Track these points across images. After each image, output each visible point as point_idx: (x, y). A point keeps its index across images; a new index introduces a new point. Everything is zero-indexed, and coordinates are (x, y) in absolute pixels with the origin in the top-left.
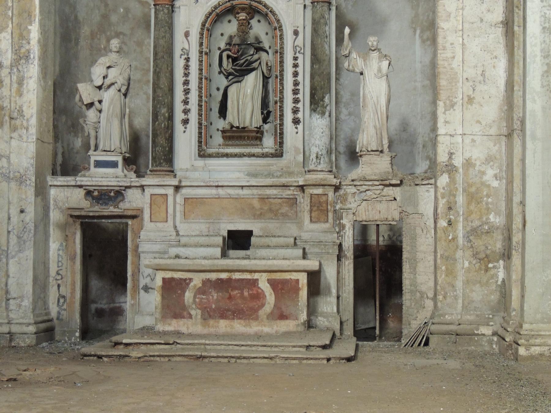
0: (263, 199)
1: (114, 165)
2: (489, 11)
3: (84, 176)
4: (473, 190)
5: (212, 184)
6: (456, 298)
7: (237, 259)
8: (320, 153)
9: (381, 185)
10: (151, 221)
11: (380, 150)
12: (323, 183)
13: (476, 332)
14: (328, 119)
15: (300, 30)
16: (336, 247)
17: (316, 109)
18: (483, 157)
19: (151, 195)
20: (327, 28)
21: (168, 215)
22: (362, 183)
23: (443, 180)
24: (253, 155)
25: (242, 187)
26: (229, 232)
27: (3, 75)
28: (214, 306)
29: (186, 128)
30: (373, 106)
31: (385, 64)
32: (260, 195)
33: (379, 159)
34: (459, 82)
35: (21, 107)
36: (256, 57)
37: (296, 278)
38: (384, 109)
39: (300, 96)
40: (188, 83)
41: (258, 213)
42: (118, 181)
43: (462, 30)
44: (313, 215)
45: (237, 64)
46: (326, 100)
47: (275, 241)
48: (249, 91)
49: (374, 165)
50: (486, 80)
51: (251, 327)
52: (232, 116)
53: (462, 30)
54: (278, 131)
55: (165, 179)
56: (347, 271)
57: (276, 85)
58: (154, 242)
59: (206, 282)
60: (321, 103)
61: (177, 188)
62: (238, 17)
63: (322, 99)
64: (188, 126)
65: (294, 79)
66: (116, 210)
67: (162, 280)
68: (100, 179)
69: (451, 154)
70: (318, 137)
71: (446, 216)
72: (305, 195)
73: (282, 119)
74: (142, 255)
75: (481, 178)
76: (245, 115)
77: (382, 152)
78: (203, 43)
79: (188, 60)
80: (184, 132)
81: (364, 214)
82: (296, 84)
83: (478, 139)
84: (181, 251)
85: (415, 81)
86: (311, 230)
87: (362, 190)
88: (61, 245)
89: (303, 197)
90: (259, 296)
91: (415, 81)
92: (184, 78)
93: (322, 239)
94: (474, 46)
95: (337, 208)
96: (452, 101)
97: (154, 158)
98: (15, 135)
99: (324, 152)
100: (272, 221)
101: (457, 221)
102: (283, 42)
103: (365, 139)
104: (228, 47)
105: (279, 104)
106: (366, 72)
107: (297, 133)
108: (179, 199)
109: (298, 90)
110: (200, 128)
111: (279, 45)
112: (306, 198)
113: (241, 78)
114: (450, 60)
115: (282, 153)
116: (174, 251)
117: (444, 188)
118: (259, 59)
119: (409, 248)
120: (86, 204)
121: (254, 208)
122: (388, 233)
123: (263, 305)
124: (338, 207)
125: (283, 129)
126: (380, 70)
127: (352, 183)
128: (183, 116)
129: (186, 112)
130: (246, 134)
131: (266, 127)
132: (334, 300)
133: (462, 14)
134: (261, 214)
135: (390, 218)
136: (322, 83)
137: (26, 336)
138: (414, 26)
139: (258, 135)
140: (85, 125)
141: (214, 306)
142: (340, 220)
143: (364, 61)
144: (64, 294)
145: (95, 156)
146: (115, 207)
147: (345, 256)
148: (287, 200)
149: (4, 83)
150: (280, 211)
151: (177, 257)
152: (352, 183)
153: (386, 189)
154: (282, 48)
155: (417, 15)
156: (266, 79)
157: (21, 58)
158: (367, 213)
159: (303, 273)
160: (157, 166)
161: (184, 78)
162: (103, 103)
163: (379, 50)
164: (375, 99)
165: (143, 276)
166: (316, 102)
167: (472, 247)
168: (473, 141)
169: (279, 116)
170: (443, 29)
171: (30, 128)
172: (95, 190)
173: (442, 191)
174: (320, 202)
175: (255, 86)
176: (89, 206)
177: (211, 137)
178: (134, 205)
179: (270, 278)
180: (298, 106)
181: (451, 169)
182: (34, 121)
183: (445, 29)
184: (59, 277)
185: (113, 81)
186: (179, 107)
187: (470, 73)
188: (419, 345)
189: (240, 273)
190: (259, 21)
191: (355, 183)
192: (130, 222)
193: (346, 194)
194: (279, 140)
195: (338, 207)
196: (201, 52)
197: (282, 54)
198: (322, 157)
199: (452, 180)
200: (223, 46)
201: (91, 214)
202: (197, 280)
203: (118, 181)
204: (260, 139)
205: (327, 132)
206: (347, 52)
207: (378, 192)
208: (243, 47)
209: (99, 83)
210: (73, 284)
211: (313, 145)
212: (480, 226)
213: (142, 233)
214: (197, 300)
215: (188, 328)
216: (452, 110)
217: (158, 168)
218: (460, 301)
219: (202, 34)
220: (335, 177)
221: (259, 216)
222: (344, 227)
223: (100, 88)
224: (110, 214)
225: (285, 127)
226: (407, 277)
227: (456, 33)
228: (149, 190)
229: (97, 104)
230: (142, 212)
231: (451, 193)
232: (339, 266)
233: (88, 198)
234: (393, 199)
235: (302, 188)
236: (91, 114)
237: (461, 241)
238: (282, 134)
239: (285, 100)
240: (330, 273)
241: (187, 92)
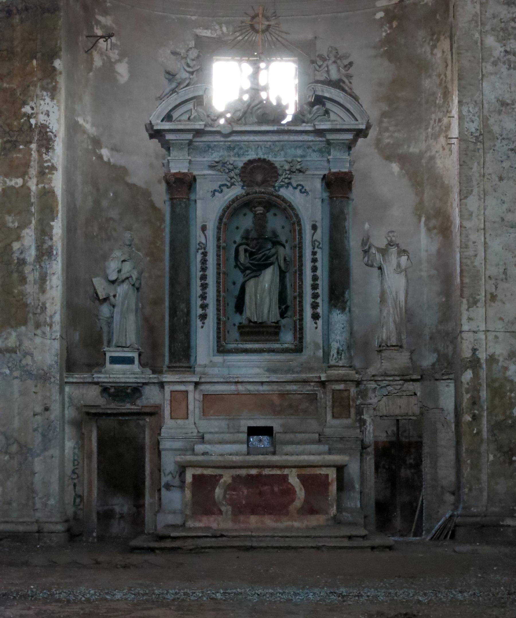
0: (283, 395)
1: (129, 361)
2: (510, 211)
3: (100, 372)
4: (497, 385)
5: (231, 380)
6: (481, 490)
8: (341, 349)
9: (401, 380)
10: (171, 418)
12: (345, 378)
13: (501, 523)
14: (348, 314)
15: (318, 224)
16: (359, 442)
18: (505, 353)
19: (171, 391)
21: (189, 412)
23: (468, 375)
25: (262, 383)
27: (26, 272)
28: (244, 502)
29: (203, 323)
32: (279, 391)
33: (398, 354)
34: (481, 279)
35: (44, 304)
36: (273, 251)
37: (326, 473)
40: (206, 278)
42: (136, 378)
43: (484, 229)
44: (335, 410)
48: (267, 286)
49: (394, 361)
50: (508, 278)
51: (281, 522)
52: (250, 312)
53: (484, 229)
54: (298, 326)
55: (186, 376)
57: (295, 279)
59: (236, 478)
60: (342, 298)
62: (256, 211)
64: (206, 321)
66: (133, 407)
67: (191, 476)
69: (474, 350)
70: (339, 333)
71: (471, 410)
73: (301, 315)
74: (163, 453)
75: (504, 373)
77: (401, 347)
78: (220, 237)
79: (205, 254)
80: (202, 327)
81: (384, 409)
82: (315, 278)
83: (501, 335)
85: (421, 270)
86: (334, 425)
88: (77, 443)
89: (325, 393)
90: (290, 491)
91: (421, 270)
92: (201, 273)
94: (496, 245)
96: (474, 298)
97: (172, 355)
98: (39, 332)
99: (345, 348)
100: (293, 417)
101: (481, 416)
102: (302, 237)
104: (244, 241)
105: (298, 299)
107: (316, 328)
108: (199, 396)
109: (318, 285)
110: (218, 324)
111: (297, 240)
112: (328, 394)
114: (472, 258)
115: (302, 348)
117: (468, 384)
120: (101, 401)
123: (293, 500)
125: (302, 324)
126: (399, 265)
127: (372, 378)
128: (200, 311)
129: (204, 307)
130: (265, 329)
131: (284, 322)
132: (358, 496)
133: (484, 213)
135: (410, 413)
137: (53, 535)
138: (418, 213)
139: (276, 330)
140: (97, 320)
141: (244, 502)
143: (383, 256)
144: (80, 493)
145: (112, 352)
146: (132, 405)
149: (28, 280)
150: (300, 407)
152: (372, 378)
153: (406, 385)
154: (301, 243)
155: (421, 202)
157: (43, 255)
158: (387, 408)
159: (333, 469)
160: (175, 362)
161: (201, 273)
164: (394, 294)
165: (164, 474)
167: (496, 440)
168: (496, 337)
169: (298, 311)
170: (466, 227)
171: (54, 325)
172: (112, 386)
173: (467, 386)
176: (105, 403)
177: (228, 332)
178: (152, 402)
179: (300, 473)
181: (474, 363)
182: (57, 318)
183: (467, 228)
184: (75, 476)
185: (128, 275)
186: (196, 302)
187: (493, 271)
188: (446, 537)
189: (270, 469)
190: (275, 215)
193: (366, 390)
194: (298, 336)
195: (358, 402)
196: (218, 247)
197: (301, 248)
198: (343, 352)
199: (476, 375)
200: (238, 239)
201: (109, 412)
202: (227, 477)
203: (136, 378)
204: (277, 334)
207: (399, 387)
208: (260, 241)
209: (113, 276)
210: (90, 483)
211: (334, 340)
212: (504, 420)
214: (227, 496)
215: (218, 524)
216: (475, 306)
217: (178, 364)
218: (485, 494)
219: (219, 228)
220: (356, 373)
221: (278, 411)
223: (113, 282)
224: (128, 411)
227: (478, 231)
228: (168, 386)
229: (112, 298)
230: (160, 409)
231: (475, 388)
232: (361, 461)
234: (413, 394)
235: (323, 384)
236: (105, 309)
237: (485, 435)
238: (301, 329)
240: (354, 469)
241: (204, 286)
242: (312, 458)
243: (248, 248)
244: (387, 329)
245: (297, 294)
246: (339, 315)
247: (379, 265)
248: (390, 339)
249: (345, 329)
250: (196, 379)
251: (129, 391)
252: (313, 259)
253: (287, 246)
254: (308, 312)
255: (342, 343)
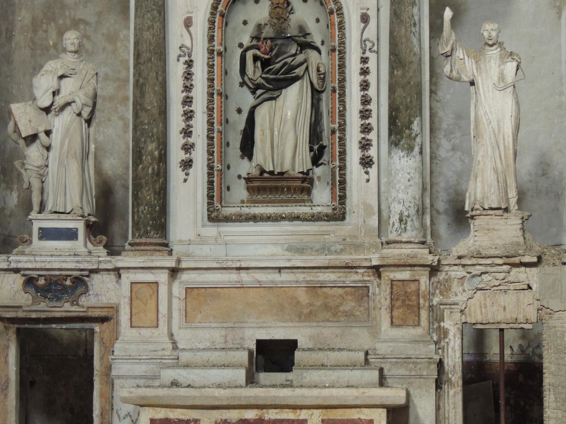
0: (313, 288)
1: (71, 235)
3: (23, 253)
5: (230, 264)
7: (272, 387)
8: (406, 214)
10: (131, 327)
11: (503, 207)
12: (410, 261)
14: (418, 158)
15: (372, 14)
16: (434, 367)
17: (399, 141)
19: (132, 283)
20: (415, 10)
21: (160, 316)
22: (474, 261)
24: (297, 218)
25: (280, 269)
26: (260, 343)
29: (187, 174)
30: (492, 136)
31: (511, 66)
32: (308, 282)
33: (502, 222)
36: (300, 58)
37: (369, 418)
38: (510, 140)
39: (372, 121)
40: (191, 102)
41: (306, 311)
42: (78, 262)
44: (395, 313)
45: (270, 70)
46: (415, 126)
47: (333, 356)
48: (289, 114)
49: (495, 232)
52: (262, 155)
54: (338, 178)
55: (154, 258)
56: (452, 406)
57: (333, 103)
58: (138, 360)
60: (407, 131)
61: (174, 272)
63: (409, 125)
64: (191, 171)
65: (362, 93)
66: (74, 308)
68: (49, 259)
70: (403, 187)
72: (383, 282)
73: (343, 159)
74: (116, 382)
76: (283, 152)
77: (506, 210)
78: (213, 36)
79: (189, 64)
80: (185, 181)
82: (366, 101)
84: (181, 375)
86: (393, 339)
87: (475, 273)
89: (379, 285)
92: (185, 94)
93: (411, 353)
95: (435, 302)
97: (136, 224)
99: (412, 211)
103: (479, 190)
104: (254, 43)
105: (337, 135)
106: (479, 81)
107: (368, 181)
108: (178, 289)
110: (210, 174)
111: (337, 38)
112: (383, 287)
113: (276, 93)
115: (344, 213)
116: (169, 375)
118: (306, 61)
119: (553, 368)
120: (24, 299)
121: (298, 302)
122: (520, 342)
124: (436, 301)
125: (345, 174)
126: (502, 77)
127: (458, 262)
128: (183, 156)
129: (188, 148)
130: (285, 184)
131: (318, 171)
134: (311, 312)
135: (521, 319)
136: (409, 100)
138: (558, 4)
139: (305, 185)
140: (23, 171)
142: (439, 322)
146: (72, 304)
147: (449, 380)
148: (353, 290)
150: (341, 309)
151: (175, 384)
153: (515, 270)
154: (342, 43)
156: (316, 93)
158: (484, 310)
160: (140, 236)
161: (185, 94)
162: (53, 135)
163: (501, 44)
164: (494, 124)
165: (119, 416)
166: (399, 131)
169: (338, 154)
172: (40, 276)
174: (406, 293)
175: (299, 105)
176: (30, 302)
177: (228, 189)
178: (104, 300)
179: (326, 418)
180: (369, 137)
185: (69, 99)
186: (176, 141)
189: (277, 411)
191: (464, 261)
192: (97, 328)
193: (448, 280)
194: (338, 193)
195: (436, 301)
197: (342, 53)
198: (409, 220)
200: (246, 41)
201: (34, 316)
203: (78, 262)
204: (308, 191)
205: (417, 179)
206: (448, 49)
207: (502, 275)
208: (279, 42)
209: (46, 103)
213: (117, 346)
217: (143, 240)
219: (212, 22)
220: (430, 253)
221: (306, 316)
222: (445, 333)
223: (47, 110)
224: (64, 314)
225: (348, 172)
226: (552, 415)
228: (127, 275)
229: (42, 136)
230: (117, 311)
232: (438, 398)
233: (28, 289)
234: (526, 287)
235: (377, 270)
236: (34, 153)
238: (343, 182)
239: (348, 128)
241: (189, 116)
242: (353, 392)
243: (258, 53)
244: (483, 183)
245: (337, 126)
246: (402, 159)
247: (472, 78)
248: (487, 198)
249: (412, 182)
250: (173, 264)
251: (68, 283)
252: (362, 69)
253: (323, 49)
254: (354, 154)
255: (407, 204)
